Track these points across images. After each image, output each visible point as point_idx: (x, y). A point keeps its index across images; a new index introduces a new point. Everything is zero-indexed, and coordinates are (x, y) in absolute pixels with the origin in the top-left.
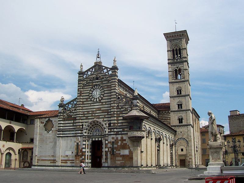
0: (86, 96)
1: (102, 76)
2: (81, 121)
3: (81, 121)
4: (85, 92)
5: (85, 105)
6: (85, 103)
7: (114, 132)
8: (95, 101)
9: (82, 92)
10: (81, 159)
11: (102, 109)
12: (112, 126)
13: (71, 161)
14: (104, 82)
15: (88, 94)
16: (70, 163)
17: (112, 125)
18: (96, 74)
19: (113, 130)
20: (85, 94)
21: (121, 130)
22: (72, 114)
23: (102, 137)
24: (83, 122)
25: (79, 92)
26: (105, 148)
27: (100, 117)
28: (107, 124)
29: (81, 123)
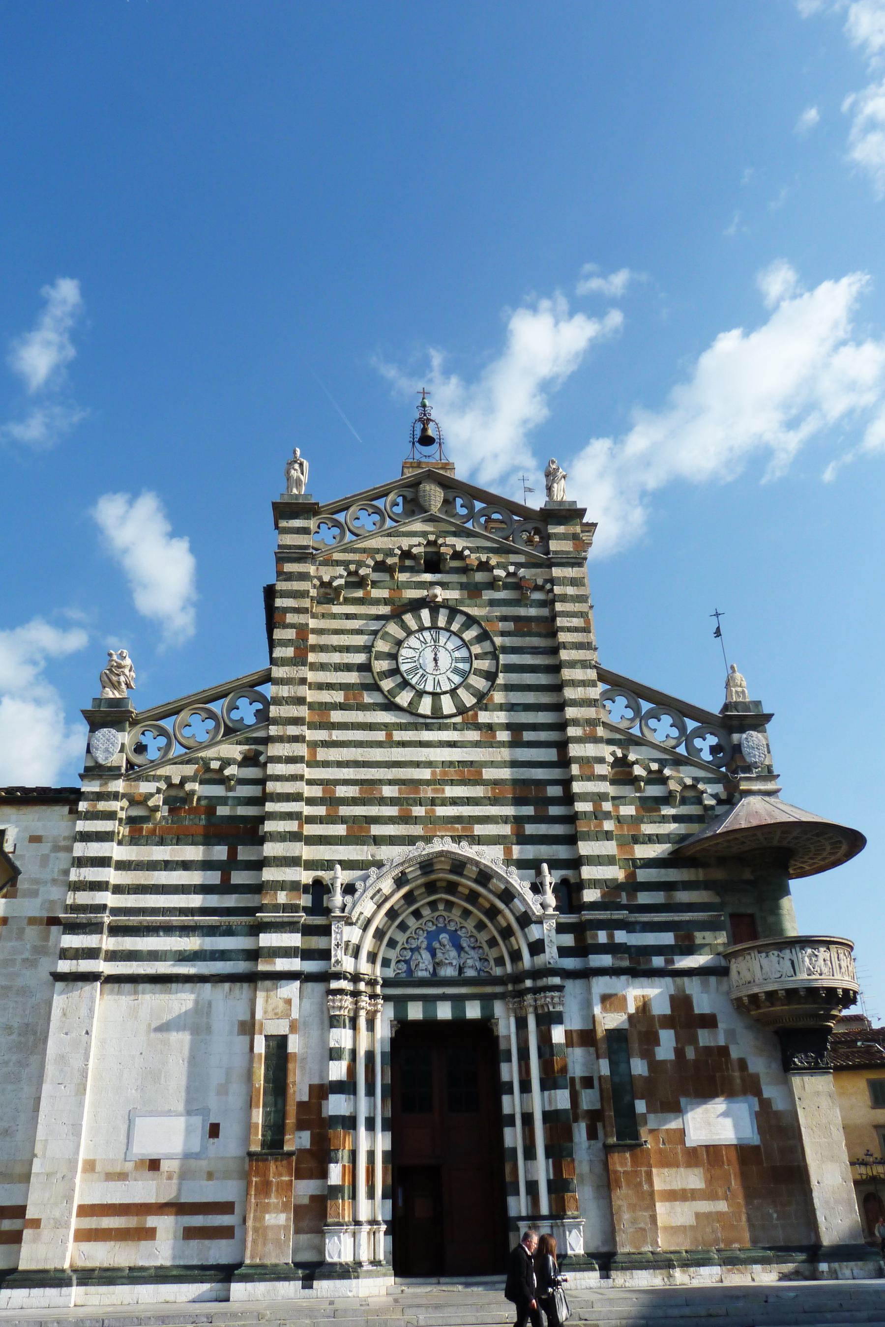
0: (348, 668)
1: (477, 550)
2: (307, 852)
3: (307, 852)
4: (336, 640)
5: (337, 735)
6: (336, 716)
7: (612, 948)
8: (425, 706)
9: (312, 639)
10: (305, 1189)
11: (488, 774)
12: (593, 906)
13: (198, 1221)
14: (487, 595)
15: (360, 658)
16: (190, 1233)
17: (590, 895)
18: (424, 534)
19: (602, 937)
20: (336, 658)
21: (667, 938)
22: (218, 791)
23: (495, 996)
24: (328, 865)
25: (290, 634)
26: (549, 1083)
27: (479, 830)
28: (549, 890)
29: (310, 865)
